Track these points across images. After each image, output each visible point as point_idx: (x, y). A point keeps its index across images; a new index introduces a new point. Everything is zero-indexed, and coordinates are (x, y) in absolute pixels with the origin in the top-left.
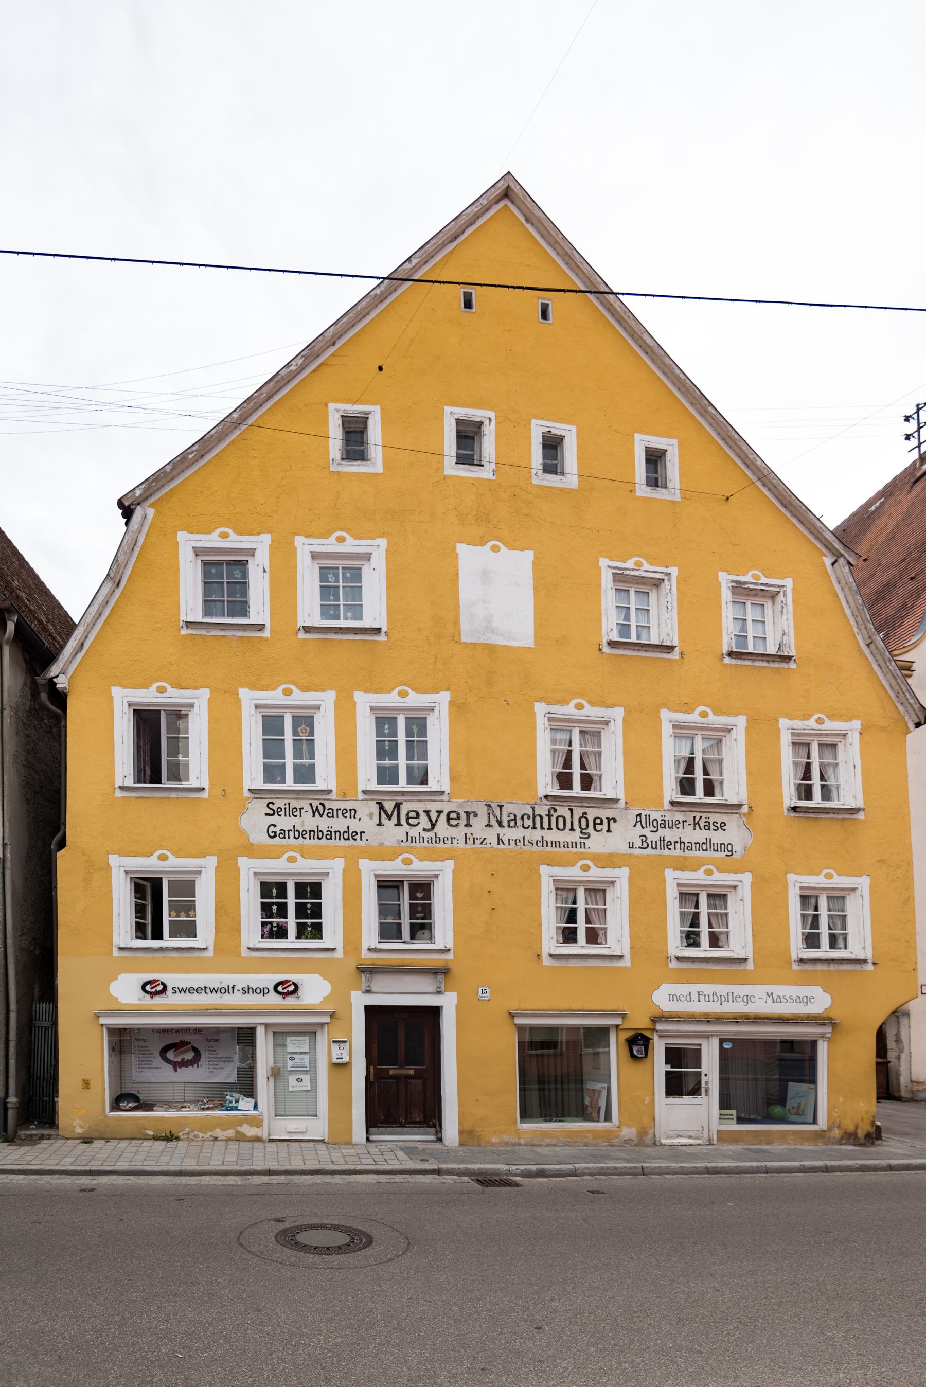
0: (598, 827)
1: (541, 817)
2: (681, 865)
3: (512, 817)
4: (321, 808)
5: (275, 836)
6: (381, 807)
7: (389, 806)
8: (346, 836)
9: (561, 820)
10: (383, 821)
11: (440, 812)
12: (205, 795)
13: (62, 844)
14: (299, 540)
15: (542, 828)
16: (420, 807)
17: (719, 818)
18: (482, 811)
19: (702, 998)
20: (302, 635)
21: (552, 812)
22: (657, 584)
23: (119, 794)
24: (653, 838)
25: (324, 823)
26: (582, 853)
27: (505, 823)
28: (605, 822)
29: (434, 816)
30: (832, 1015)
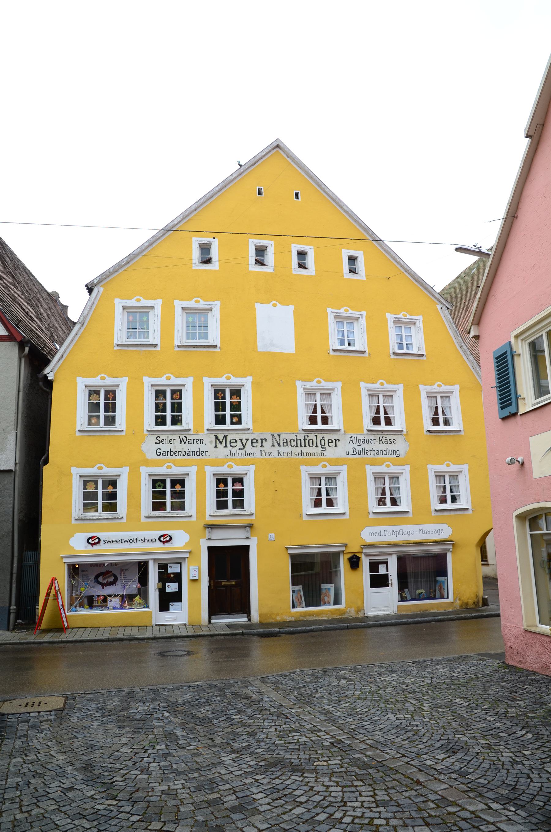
0: (330, 444)
1: (300, 440)
2: (373, 463)
3: (285, 441)
4: (185, 439)
5: (160, 455)
6: (217, 438)
7: (221, 437)
8: (198, 454)
9: (311, 441)
10: (217, 446)
11: (247, 439)
12: (124, 434)
13: (46, 462)
14: (176, 302)
15: (301, 446)
16: (237, 437)
17: (392, 437)
18: (270, 439)
19: (386, 533)
20: (177, 349)
21: (306, 437)
22: (357, 319)
23: (78, 434)
24: (359, 449)
25: (186, 447)
26: (322, 459)
27: (281, 444)
28: (334, 441)
29: (244, 442)
30: (452, 539)
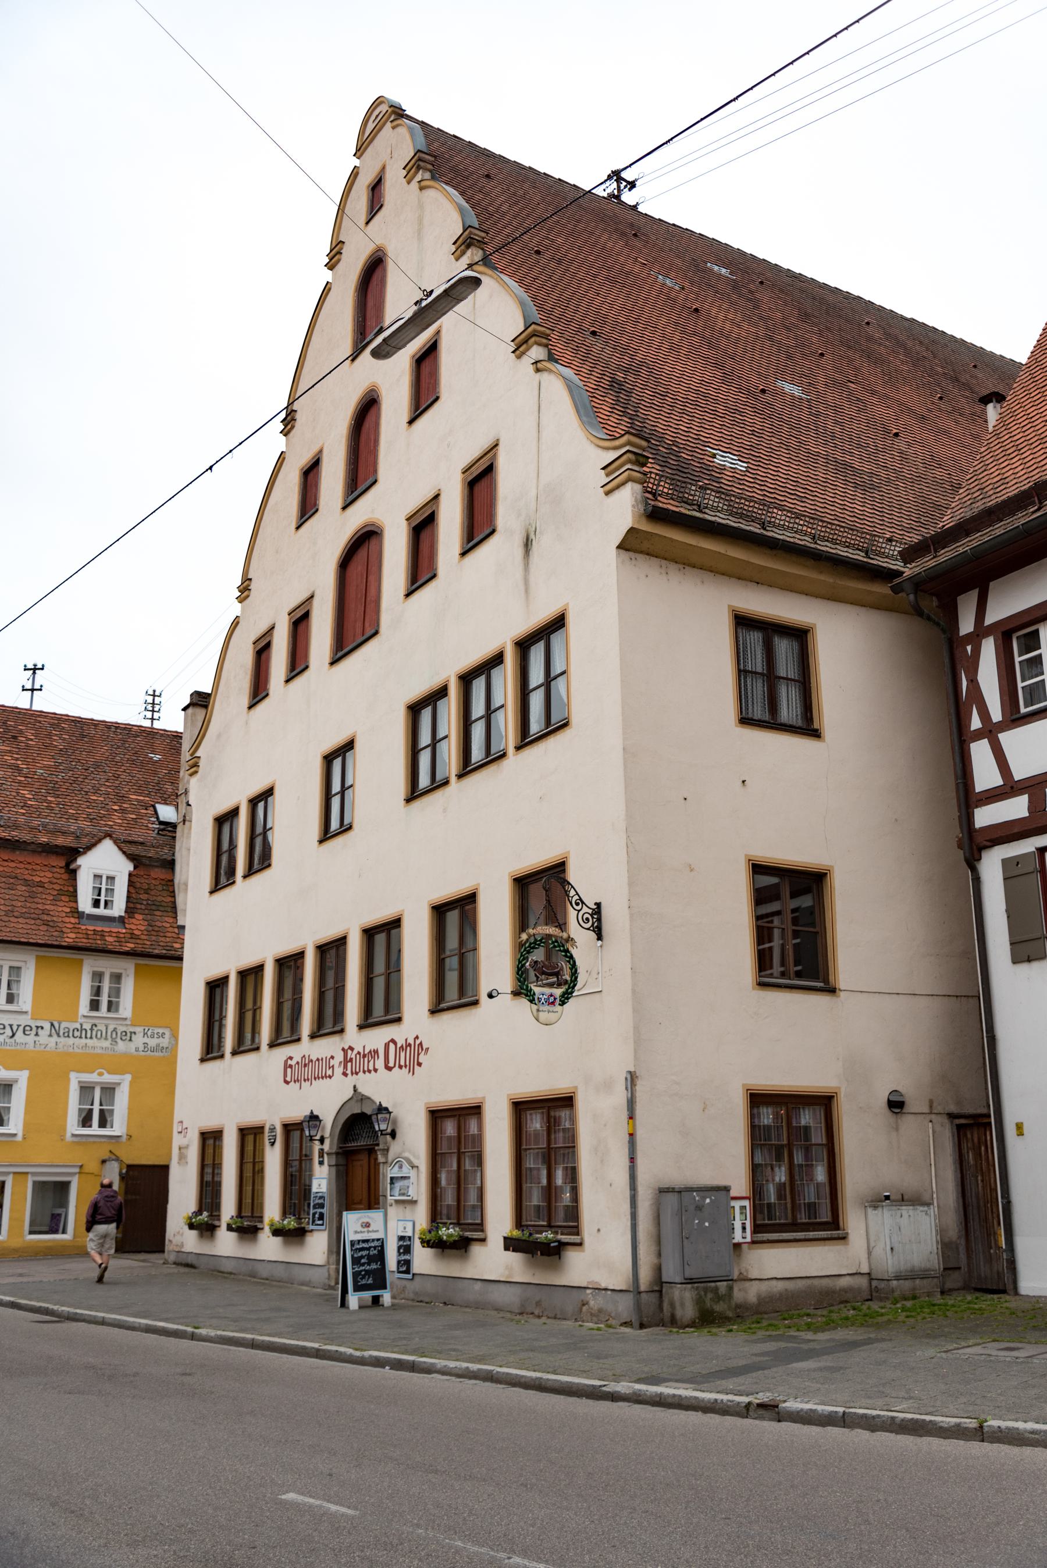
11: (19, 1026)
18: (47, 1026)
